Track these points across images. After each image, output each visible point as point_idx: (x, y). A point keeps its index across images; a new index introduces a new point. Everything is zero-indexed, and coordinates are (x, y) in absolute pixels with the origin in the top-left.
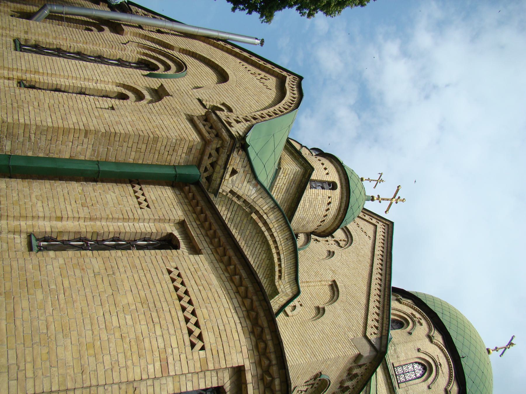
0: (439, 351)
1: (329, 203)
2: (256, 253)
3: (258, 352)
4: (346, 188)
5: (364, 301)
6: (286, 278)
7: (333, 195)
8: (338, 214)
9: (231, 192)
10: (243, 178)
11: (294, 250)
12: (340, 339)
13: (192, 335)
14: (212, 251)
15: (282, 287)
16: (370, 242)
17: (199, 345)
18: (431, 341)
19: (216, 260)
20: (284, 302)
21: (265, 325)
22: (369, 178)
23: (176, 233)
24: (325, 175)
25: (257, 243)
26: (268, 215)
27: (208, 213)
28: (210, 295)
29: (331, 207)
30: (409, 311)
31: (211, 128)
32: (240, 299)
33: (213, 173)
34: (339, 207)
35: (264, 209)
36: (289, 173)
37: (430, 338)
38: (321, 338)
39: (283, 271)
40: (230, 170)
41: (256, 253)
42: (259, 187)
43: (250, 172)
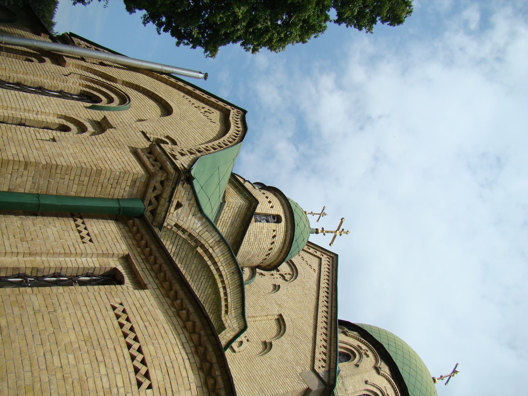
0: (386, 382)
1: (274, 237)
2: (201, 288)
3: (208, 388)
4: (291, 221)
5: (311, 334)
6: (232, 312)
7: (278, 229)
8: (283, 248)
9: (176, 225)
10: (188, 211)
11: (241, 284)
12: (288, 373)
13: (138, 373)
14: (157, 286)
15: (229, 322)
16: (315, 275)
17: (146, 383)
18: (378, 372)
19: (162, 295)
20: (231, 337)
21: (214, 360)
22: (312, 212)
23: (120, 268)
24: (270, 208)
25: (203, 278)
26: (214, 249)
27: (153, 247)
28: (156, 331)
29: (276, 240)
30: (356, 343)
31: (156, 160)
32: (187, 335)
33: (158, 206)
34: (283, 240)
35: (209, 242)
36: (233, 206)
37: (377, 370)
38: (269, 373)
39: (229, 305)
40: (175, 203)
41: (201, 288)
42: (204, 220)
43: (195, 205)
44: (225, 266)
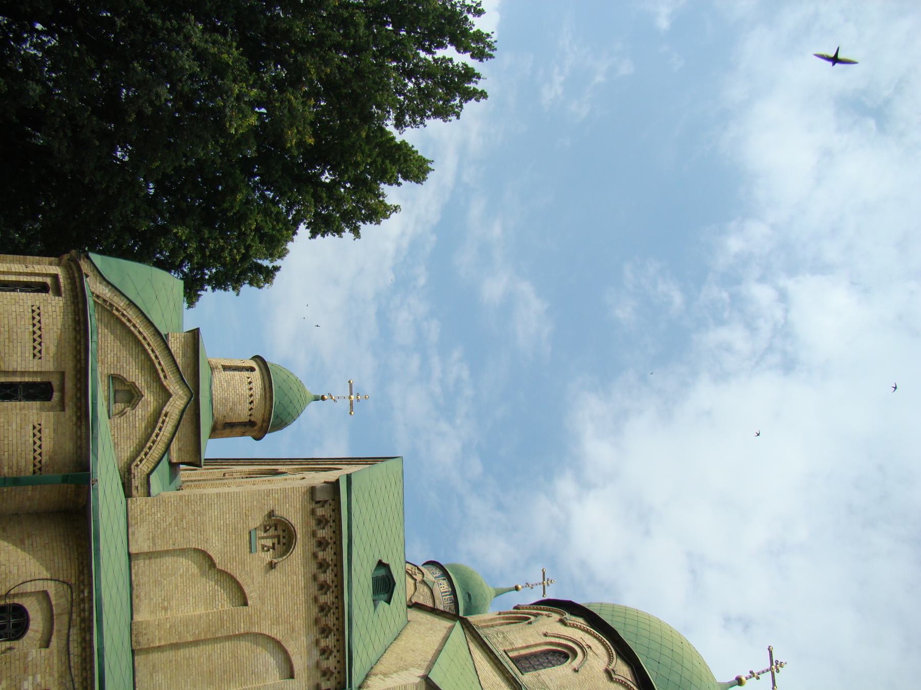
2: (134, 353)
6: (170, 375)
10: (95, 280)
15: (172, 388)
20: (182, 406)
35: (121, 305)
39: (165, 369)
41: (134, 353)
42: (110, 287)
44: (136, 319)
